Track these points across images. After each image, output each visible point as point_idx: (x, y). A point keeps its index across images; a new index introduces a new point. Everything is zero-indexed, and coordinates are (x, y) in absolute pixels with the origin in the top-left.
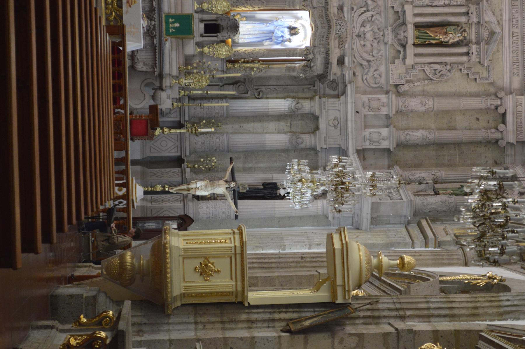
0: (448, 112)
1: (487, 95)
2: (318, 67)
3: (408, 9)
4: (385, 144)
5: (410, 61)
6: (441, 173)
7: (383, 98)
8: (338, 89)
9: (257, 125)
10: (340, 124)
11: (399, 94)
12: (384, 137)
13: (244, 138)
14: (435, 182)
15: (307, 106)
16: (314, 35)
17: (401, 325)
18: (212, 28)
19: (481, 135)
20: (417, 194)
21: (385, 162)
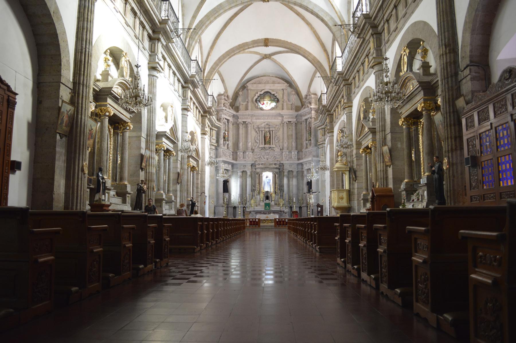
0: (288, 136)
1: (283, 126)
2: (277, 170)
3: (261, 146)
4: (296, 153)
5: (274, 146)
6: (304, 139)
7: (284, 153)
8: (282, 165)
9: (291, 187)
10: (291, 165)
11: (283, 149)
12: (294, 153)
13: (294, 190)
14: (307, 140)
15: (286, 173)
16: (269, 171)
17: (354, 156)
18: (267, 198)
19: (294, 128)
20: (310, 145)
21: (301, 153)
